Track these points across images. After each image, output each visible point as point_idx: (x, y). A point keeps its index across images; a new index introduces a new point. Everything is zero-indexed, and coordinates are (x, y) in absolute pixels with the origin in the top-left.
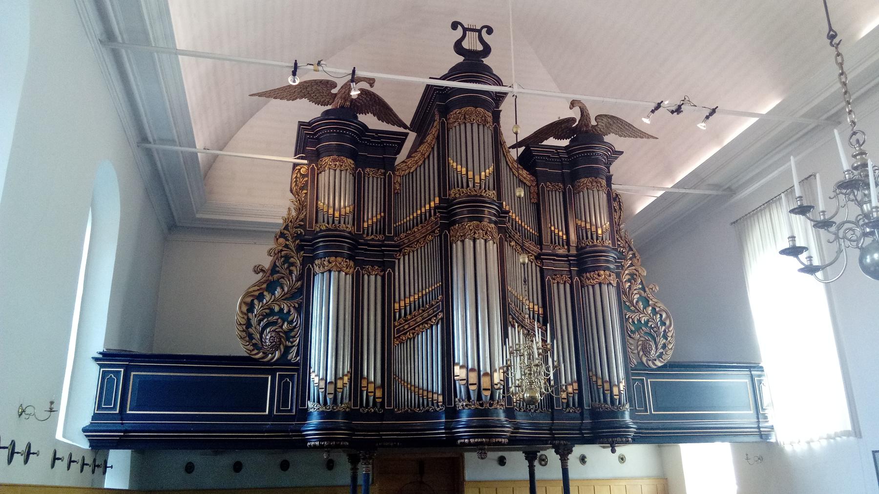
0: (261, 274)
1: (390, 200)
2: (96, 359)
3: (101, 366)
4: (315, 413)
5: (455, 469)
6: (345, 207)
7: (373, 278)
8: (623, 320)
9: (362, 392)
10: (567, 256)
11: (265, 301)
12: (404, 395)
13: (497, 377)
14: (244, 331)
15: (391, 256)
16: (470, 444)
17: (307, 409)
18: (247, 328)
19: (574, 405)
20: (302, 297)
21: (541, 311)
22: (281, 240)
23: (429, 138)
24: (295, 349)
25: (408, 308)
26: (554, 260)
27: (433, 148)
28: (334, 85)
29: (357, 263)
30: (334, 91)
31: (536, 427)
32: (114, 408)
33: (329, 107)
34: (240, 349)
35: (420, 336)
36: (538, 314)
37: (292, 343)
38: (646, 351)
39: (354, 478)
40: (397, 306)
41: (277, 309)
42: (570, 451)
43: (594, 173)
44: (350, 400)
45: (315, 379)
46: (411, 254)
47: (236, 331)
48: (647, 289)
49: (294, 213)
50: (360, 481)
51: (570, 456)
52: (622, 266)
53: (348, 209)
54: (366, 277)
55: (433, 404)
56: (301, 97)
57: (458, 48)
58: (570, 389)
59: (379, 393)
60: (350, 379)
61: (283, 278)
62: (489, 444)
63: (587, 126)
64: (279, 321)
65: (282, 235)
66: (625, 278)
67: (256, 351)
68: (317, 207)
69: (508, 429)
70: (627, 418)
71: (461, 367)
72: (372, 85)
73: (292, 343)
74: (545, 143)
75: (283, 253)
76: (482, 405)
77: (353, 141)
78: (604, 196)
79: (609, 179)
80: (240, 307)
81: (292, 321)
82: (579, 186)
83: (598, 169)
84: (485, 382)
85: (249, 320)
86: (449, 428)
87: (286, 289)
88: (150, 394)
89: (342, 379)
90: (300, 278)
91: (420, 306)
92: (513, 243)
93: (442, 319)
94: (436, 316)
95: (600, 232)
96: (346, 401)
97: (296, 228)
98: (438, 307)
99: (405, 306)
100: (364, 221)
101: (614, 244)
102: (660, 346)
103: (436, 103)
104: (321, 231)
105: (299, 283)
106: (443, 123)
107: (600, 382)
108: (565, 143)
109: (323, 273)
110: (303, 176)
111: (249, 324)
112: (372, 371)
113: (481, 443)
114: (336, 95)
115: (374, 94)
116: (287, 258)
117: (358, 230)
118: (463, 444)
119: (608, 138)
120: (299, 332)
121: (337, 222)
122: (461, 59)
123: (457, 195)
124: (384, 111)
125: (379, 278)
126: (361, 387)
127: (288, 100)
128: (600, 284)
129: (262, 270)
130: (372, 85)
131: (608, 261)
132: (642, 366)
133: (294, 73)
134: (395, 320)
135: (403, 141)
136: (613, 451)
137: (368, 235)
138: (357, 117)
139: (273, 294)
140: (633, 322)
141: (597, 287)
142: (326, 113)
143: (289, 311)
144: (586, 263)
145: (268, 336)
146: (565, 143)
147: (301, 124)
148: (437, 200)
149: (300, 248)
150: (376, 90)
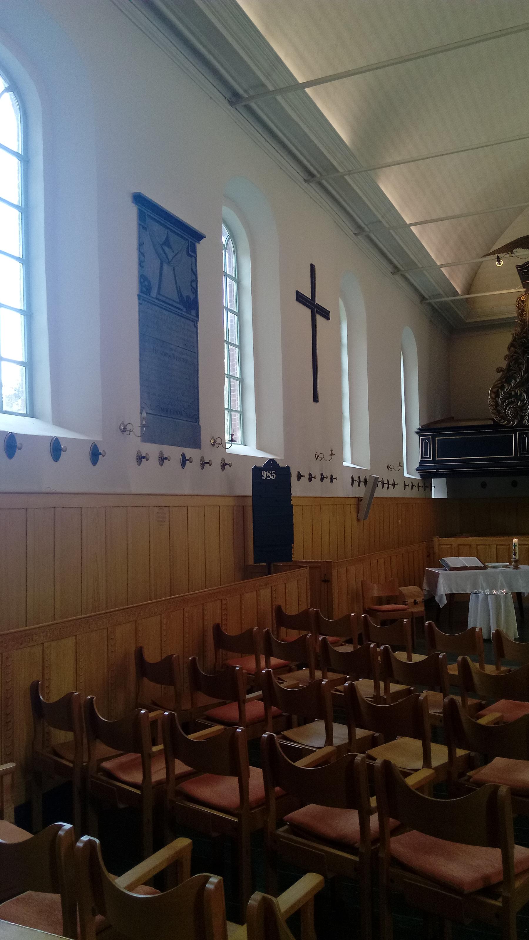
0: (501, 373)
2: (417, 433)
3: (420, 436)
14: (494, 409)
22: (512, 349)
32: (430, 458)
41: (513, 393)
61: (515, 373)
67: (503, 421)
73: (525, 413)
81: (523, 400)
87: (518, 381)
88: (446, 449)
97: (522, 338)
111: (497, 404)
116: (516, 360)
129: (501, 370)
133: (499, 261)
143: (521, 394)
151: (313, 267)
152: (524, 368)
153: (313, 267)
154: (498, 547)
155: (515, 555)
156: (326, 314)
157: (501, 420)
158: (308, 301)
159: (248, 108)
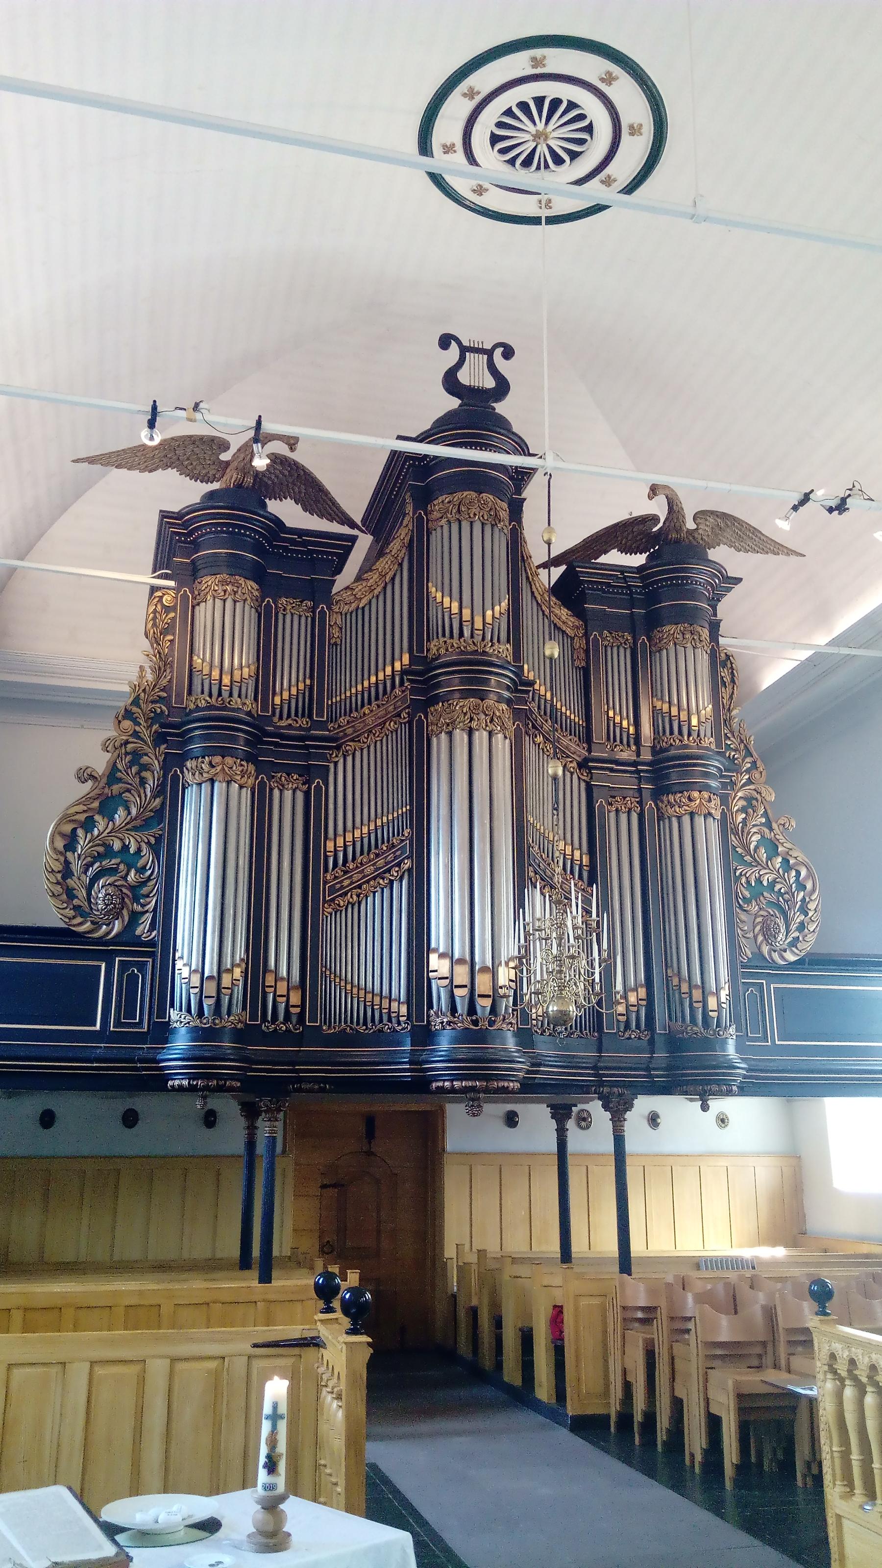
0: (90, 783)
1: (321, 656)
4: (183, 1031)
5: (428, 1133)
6: (241, 668)
7: (288, 794)
9: (265, 995)
10: (635, 764)
11: (96, 832)
13: (505, 975)
14: (58, 883)
15: (323, 757)
16: (453, 1090)
17: (168, 1023)
18: (64, 878)
19: (638, 1026)
21: (586, 860)
22: (127, 724)
23: (395, 546)
24: (149, 916)
25: (350, 850)
26: (612, 770)
27: (401, 565)
28: (224, 446)
30: (225, 457)
31: (570, 1063)
33: (216, 486)
34: (50, 914)
35: (370, 899)
36: (581, 866)
37: (143, 906)
38: (769, 934)
39: (251, 1145)
40: (330, 846)
41: (117, 845)
42: (629, 1106)
43: (687, 616)
44: (244, 1008)
45: (182, 970)
46: (358, 754)
47: (45, 883)
48: (775, 826)
49: (150, 676)
50: (261, 1148)
51: (628, 1115)
52: (733, 784)
53: (246, 671)
54: (276, 792)
55: (390, 1020)
56: (166, 467)
57: (451, 382)
58: (632, 999)
59: (295, 998)
60: (245, 973)
61: (129, 791)
62: (486, 1090)
63: (679, 530)
64: (122, 867)
65: (128, 714)
67: (79, 920)
68: (191, 665)
69: (521, 1066)
71: (442, 956)
72: (292, 448)
73: (143, 906)
74: (603, 559)
75: (130, 746)
76: (475, 1023)
77: (258, 549)
78: (704, 659)
79: (715, 628)
80: (52, 841)
81: (144, 869)
82: (661, 640)
83: (696, 608)
84: (483, 983)
85: (67, 863)
87: (134, 811)
89: (230, 971)
90: (159, 791)
91: (371, 846)
92: (539, 739)
93: (410, 870)
94: (399, 865)
95: (694, 722)
96: (237, 1009)
97: (153, 702)
98: (403, 849)
99: (345, 846)
100: (274, 694)
101: (719, 744)
102: (793, 927)
103: (409, 483)
104: (198, 709)
105: (158, 801)
106: (420, 518)
107: (685, 988)
108: (638, 560)
109: (200, 784)
110: (168, 610)
111: (67, 872)
112: (284, 959)
113: (473, 1089)
114: (228, 463)
115: (296, 463)
116: (136, 756)
117: (265, 708)
118: (441, 1090)
119: (714, 554)
120: (155, 888)
121: (225, 694)
122: (454, 403)
123: (443, 651)
124: (315, 496)
125: (300, 796)
126: (264, 986)
127: (142, 471)
128: (692, 815)
130: (292, 448)
131: (707, 775)
132: (760, 961)
134: (326, 870)
135: (348, 550)
136: (705, 1108)
137: (281, 718)
138: (264, 506)
139: (112, 819)
140: (748, 882)
141: (686, 820)
142: (211, 495)
143: (139, 850)
144: (667, 777)
145: (100, 894)
146: (638, 560)
147: (164, 515)
148: (406, 659)
149: (159, 739)
150: (299, 456)
152: (151, 784)
154: (99, 1371)
155: (271, 1467)
157: (74, 917)
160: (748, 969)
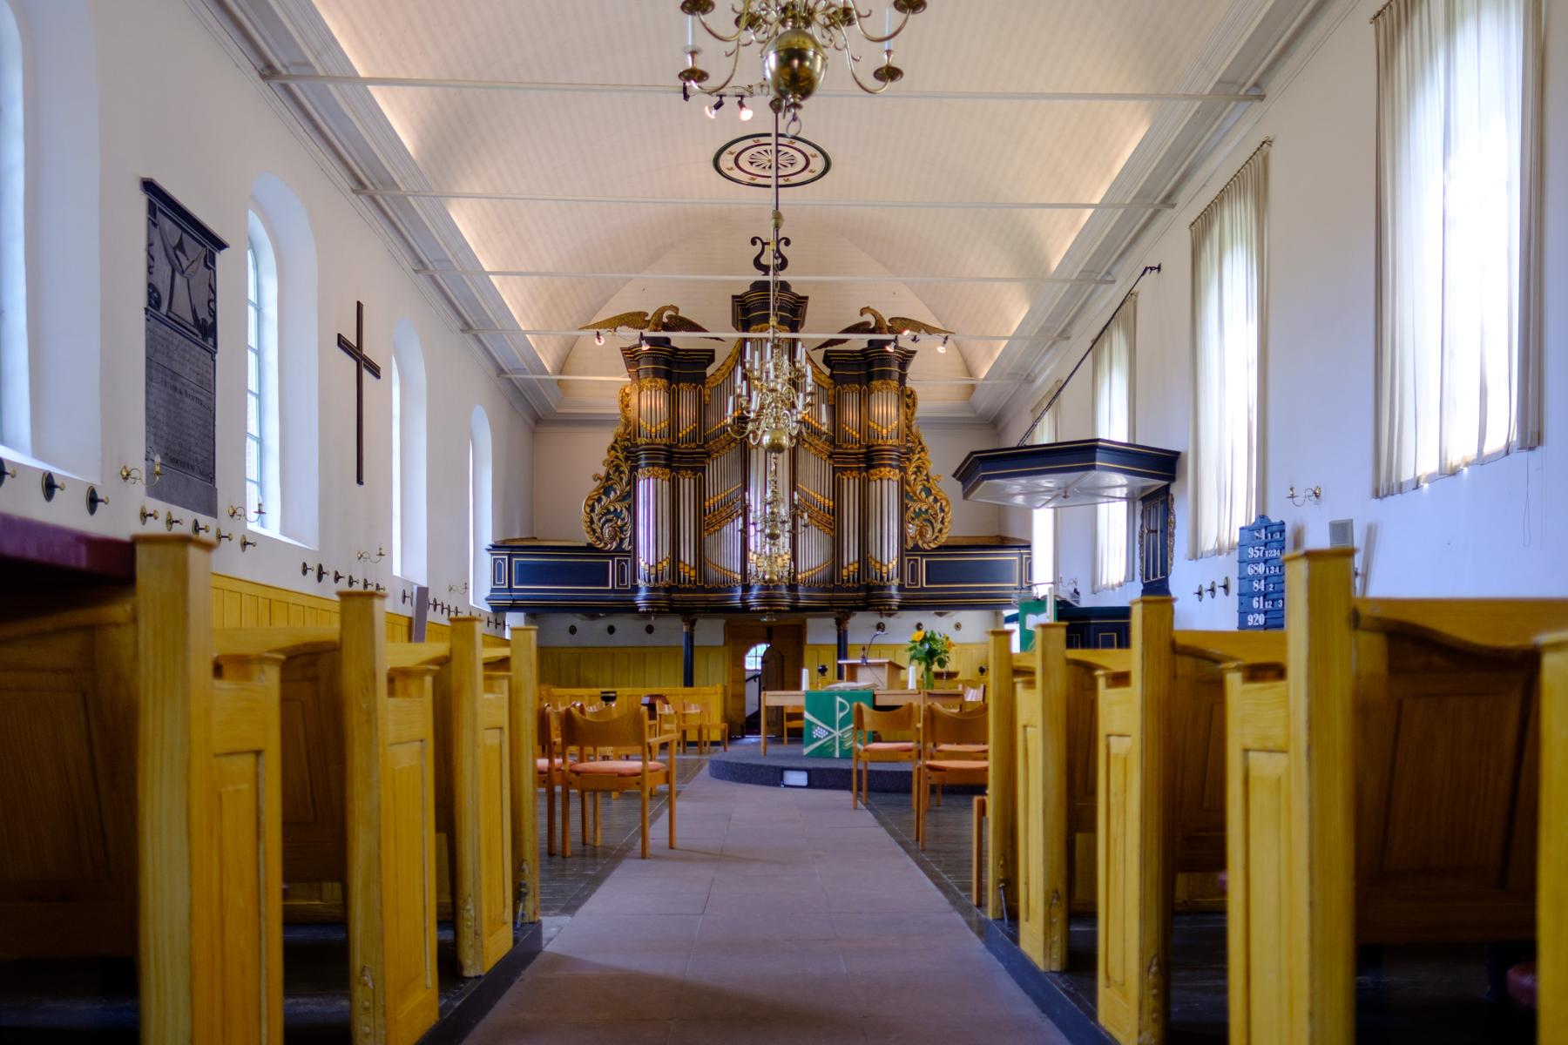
1: (702, 408)
8: (903, 508)
12: (712, 574)
20: (631, 496)
29: (672, 469)
34: (588, 539)
38: (922, 535)
43: (885, 376)
47: (584, 527)
65: (613, 448)
66: (912, 469)
69: (787, 601)
70: (894, 591)
77: (667, 362)
86: (742, 599)
90: (628, 483)
91: (726, 503)
103: (748, 311)
111: (592, 522)
112: (687, 556)
116: (617, 467)
120: (629, 527)
132: (916, 548)
149: (627, 458)
150: (681, 314)
151: (359, 305)
152: (625, 479)
153: (359, 305)
156: (375, 371)
158: (353, 349)
159: (286, 88)
160: (908, 551)
